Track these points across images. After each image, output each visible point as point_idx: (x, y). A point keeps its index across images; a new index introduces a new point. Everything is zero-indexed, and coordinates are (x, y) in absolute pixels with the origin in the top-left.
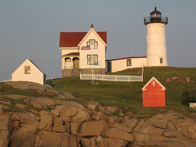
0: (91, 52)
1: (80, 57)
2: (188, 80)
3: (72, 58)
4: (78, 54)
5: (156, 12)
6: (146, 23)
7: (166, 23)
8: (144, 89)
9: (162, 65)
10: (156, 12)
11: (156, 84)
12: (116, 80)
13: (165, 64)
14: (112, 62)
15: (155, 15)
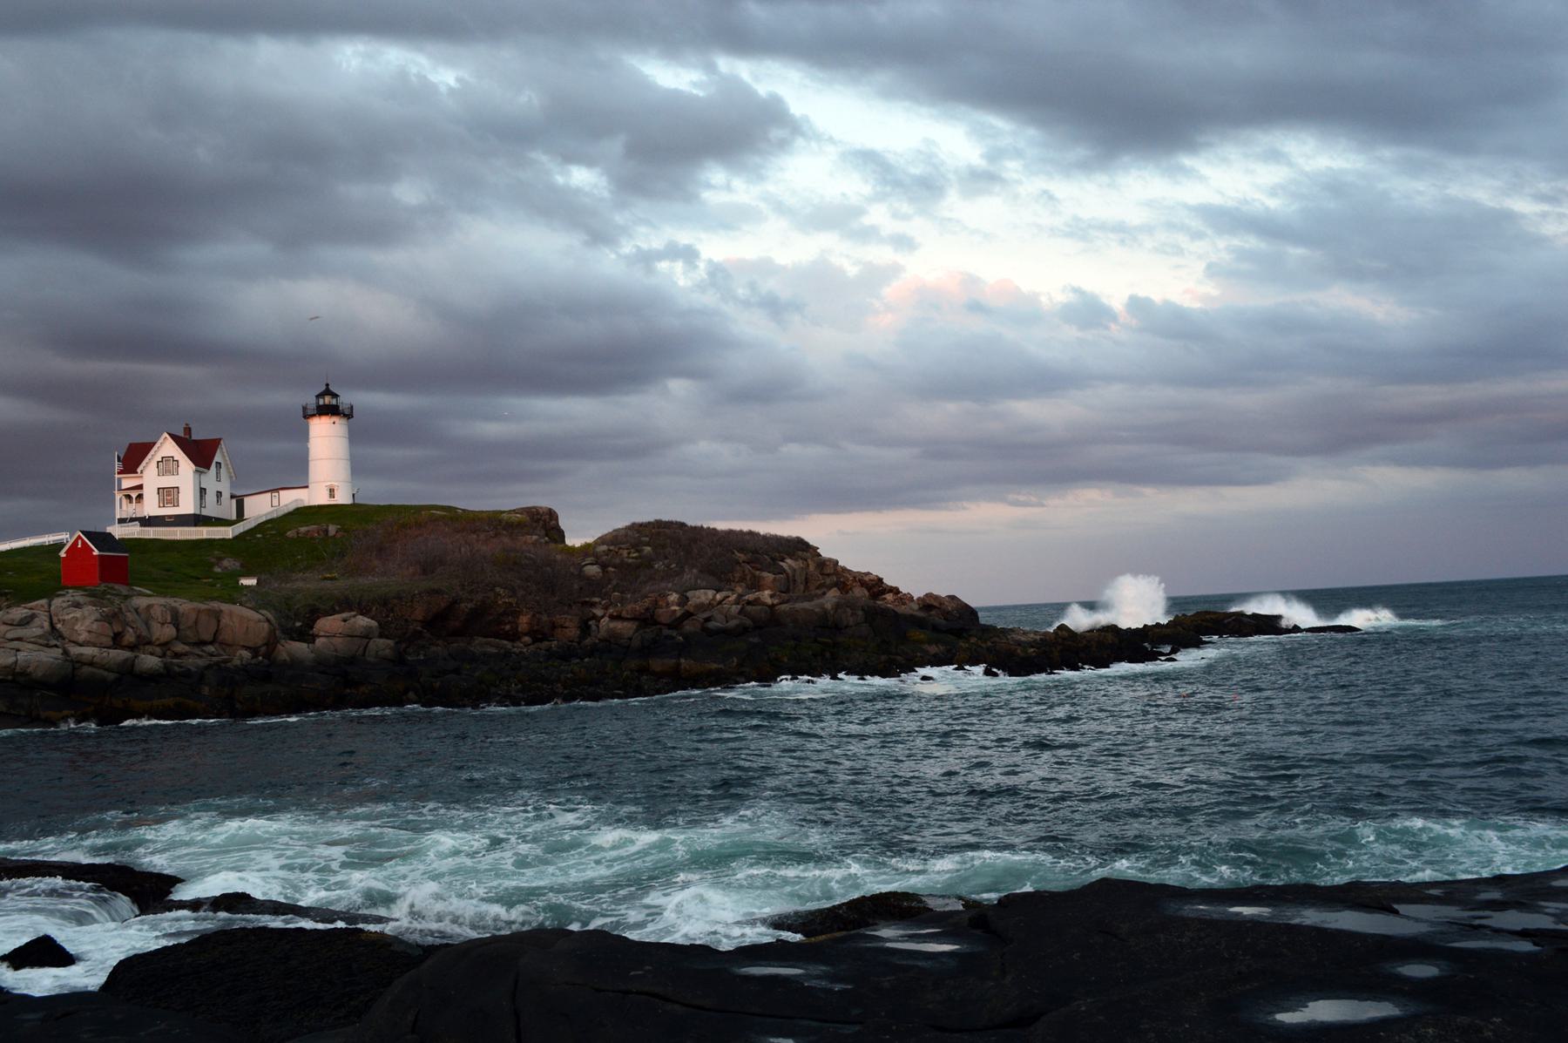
0: (168, 481)
1: (145, 492)
2: (332, 529)
3: (134, 495)
4: (140, 487)
5: (327, 392)
6: (307, 416)
7: (348, 415)
8: (63, 554)
9: (332, 502)
10: (327, 392)
11: (84, 543)
12: (178, 537)
13: (343, 498)
14: (246, 500)
15: (327, 400)
